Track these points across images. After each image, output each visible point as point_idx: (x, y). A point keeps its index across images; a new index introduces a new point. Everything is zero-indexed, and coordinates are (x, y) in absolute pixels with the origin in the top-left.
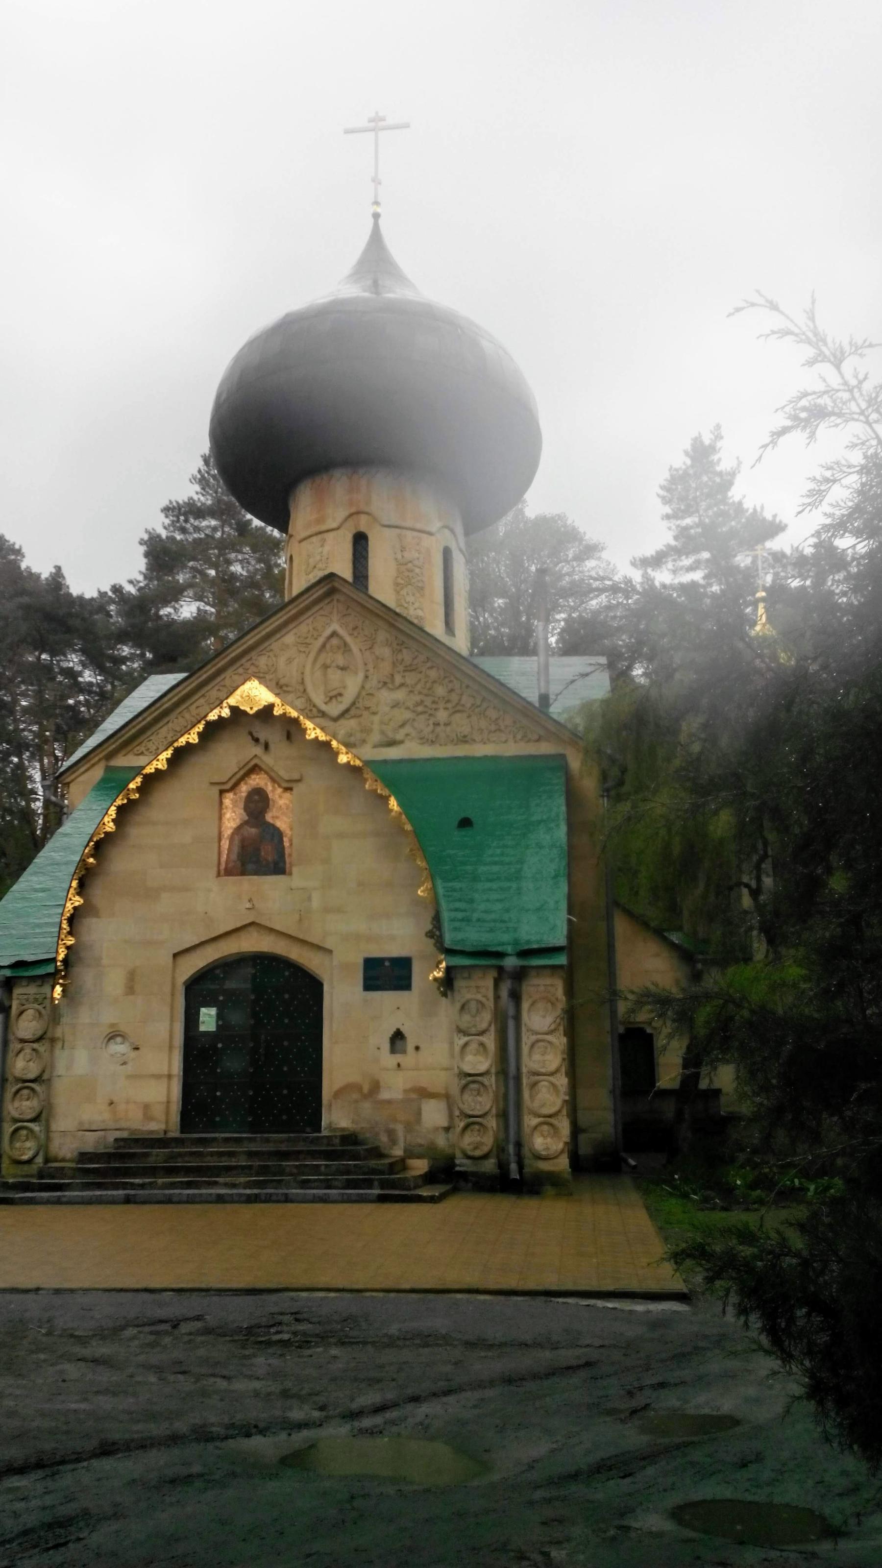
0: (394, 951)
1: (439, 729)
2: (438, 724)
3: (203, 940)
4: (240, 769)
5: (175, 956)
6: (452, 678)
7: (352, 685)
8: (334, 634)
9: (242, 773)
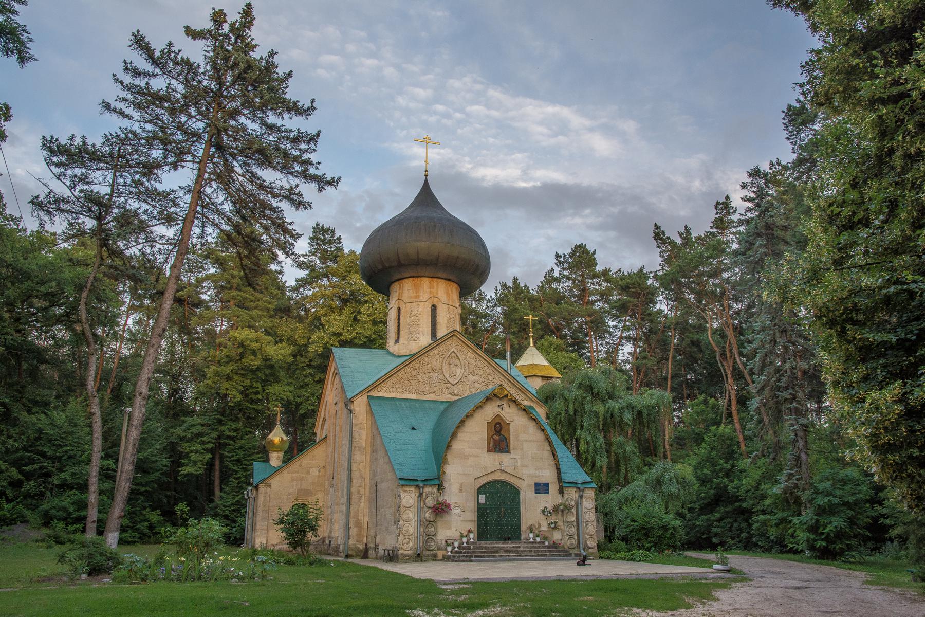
0: (544, 481)
7: (459, 372)
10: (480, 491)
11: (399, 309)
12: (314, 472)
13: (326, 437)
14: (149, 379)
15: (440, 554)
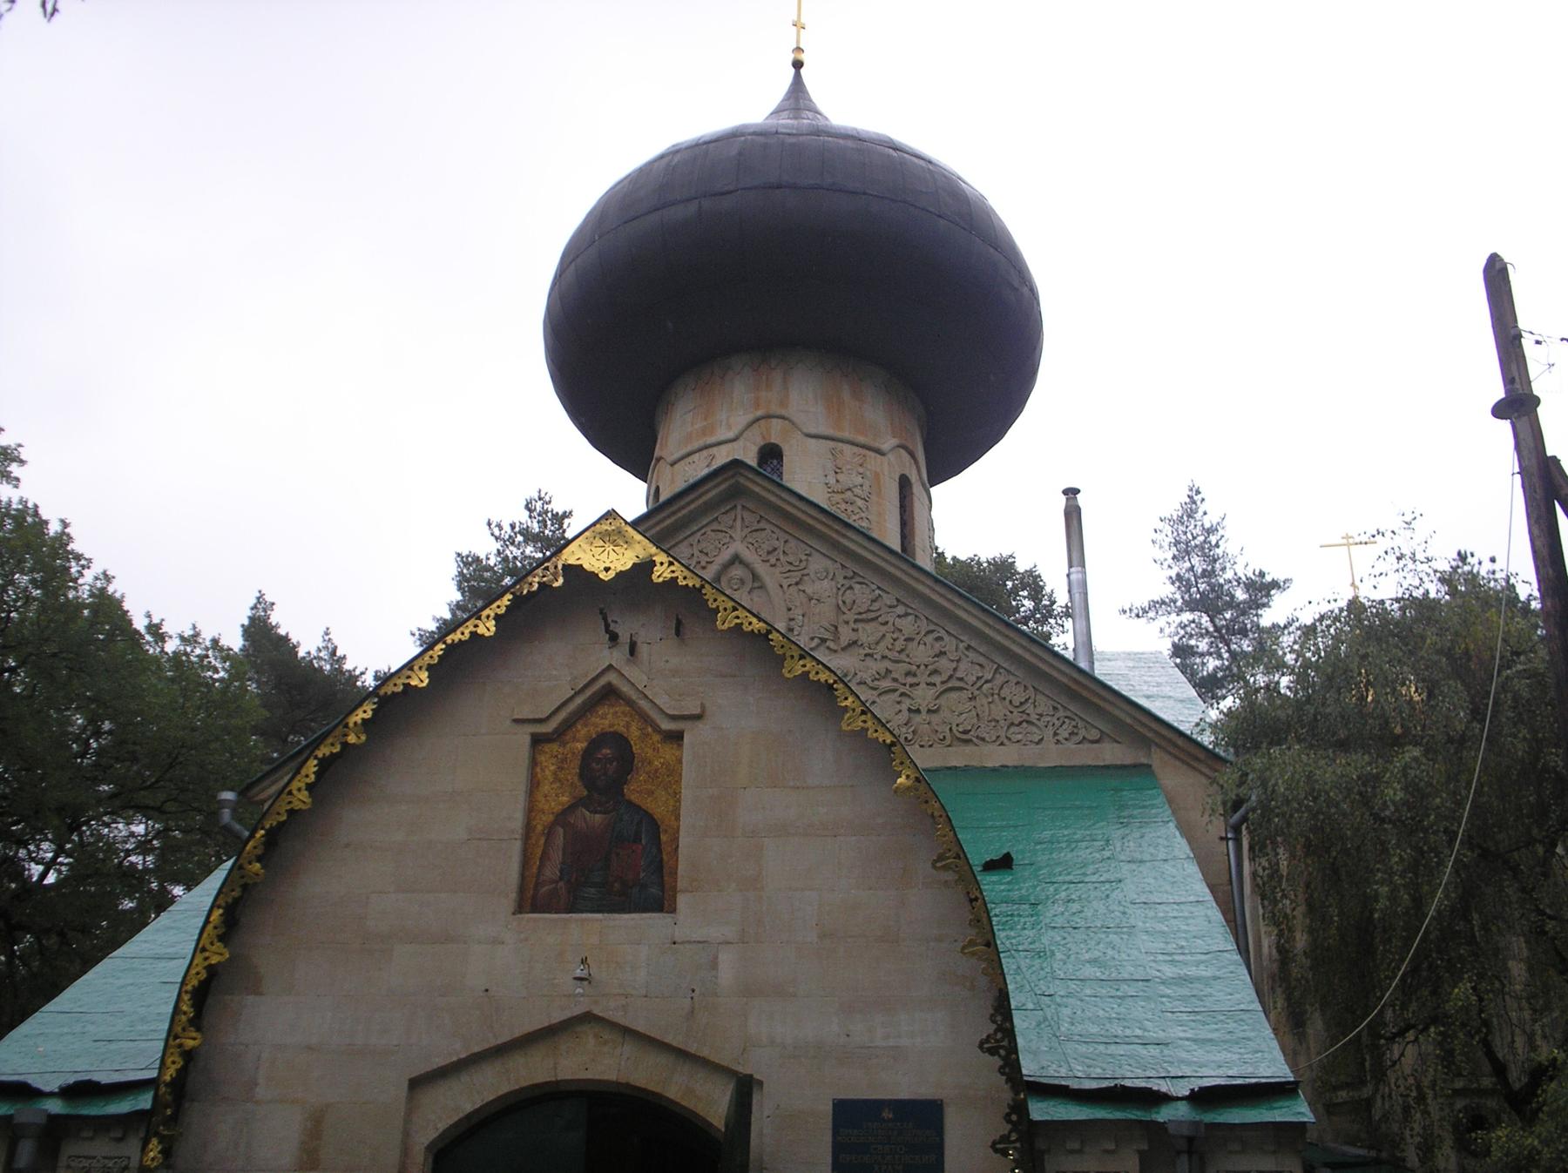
0: (902, 1085)
1: (917, 719)
2: (918, 711)
3: (476, 1049)
4: (577, 693)
5: (416, 1084)
6: (942, 633)
8: (736, 559)
9: (579, 700)
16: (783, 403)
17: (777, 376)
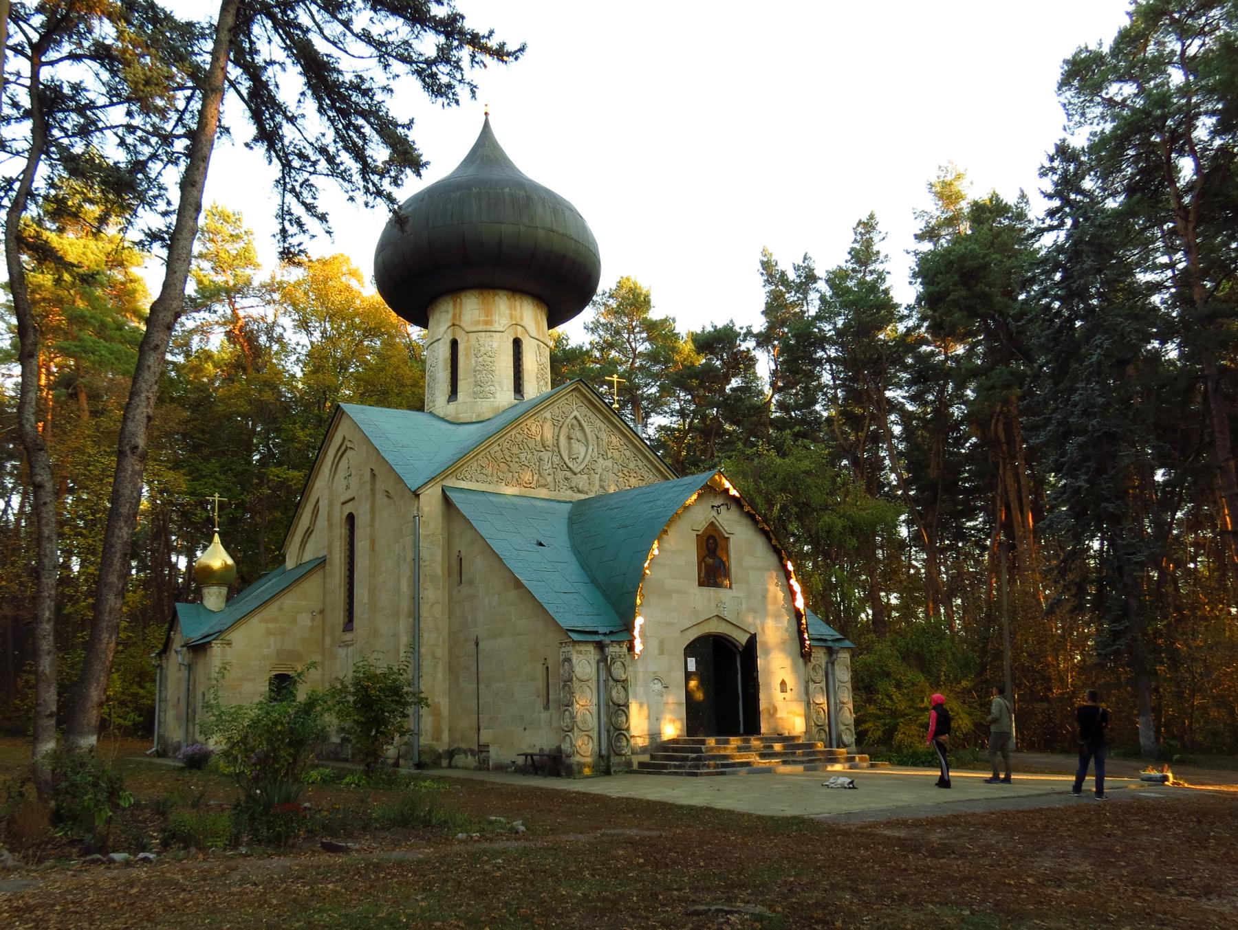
10: (690, 650)
11: (454, 344)
12: (305, 620)
13: (322, 563)
14: (149, 418)
15: (636, 760)
16: (522, 319)
17: (518, 304)
